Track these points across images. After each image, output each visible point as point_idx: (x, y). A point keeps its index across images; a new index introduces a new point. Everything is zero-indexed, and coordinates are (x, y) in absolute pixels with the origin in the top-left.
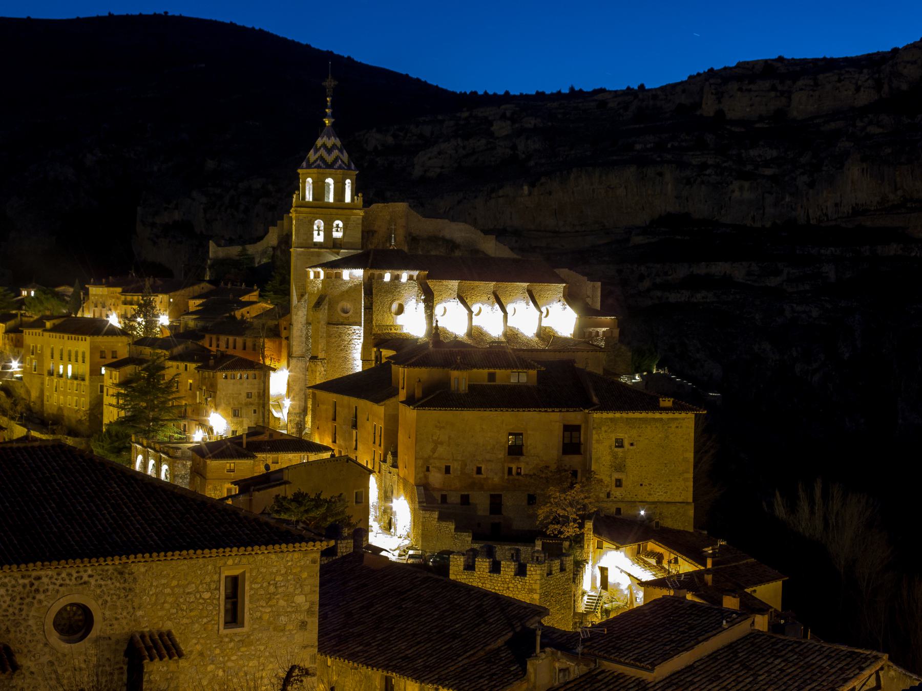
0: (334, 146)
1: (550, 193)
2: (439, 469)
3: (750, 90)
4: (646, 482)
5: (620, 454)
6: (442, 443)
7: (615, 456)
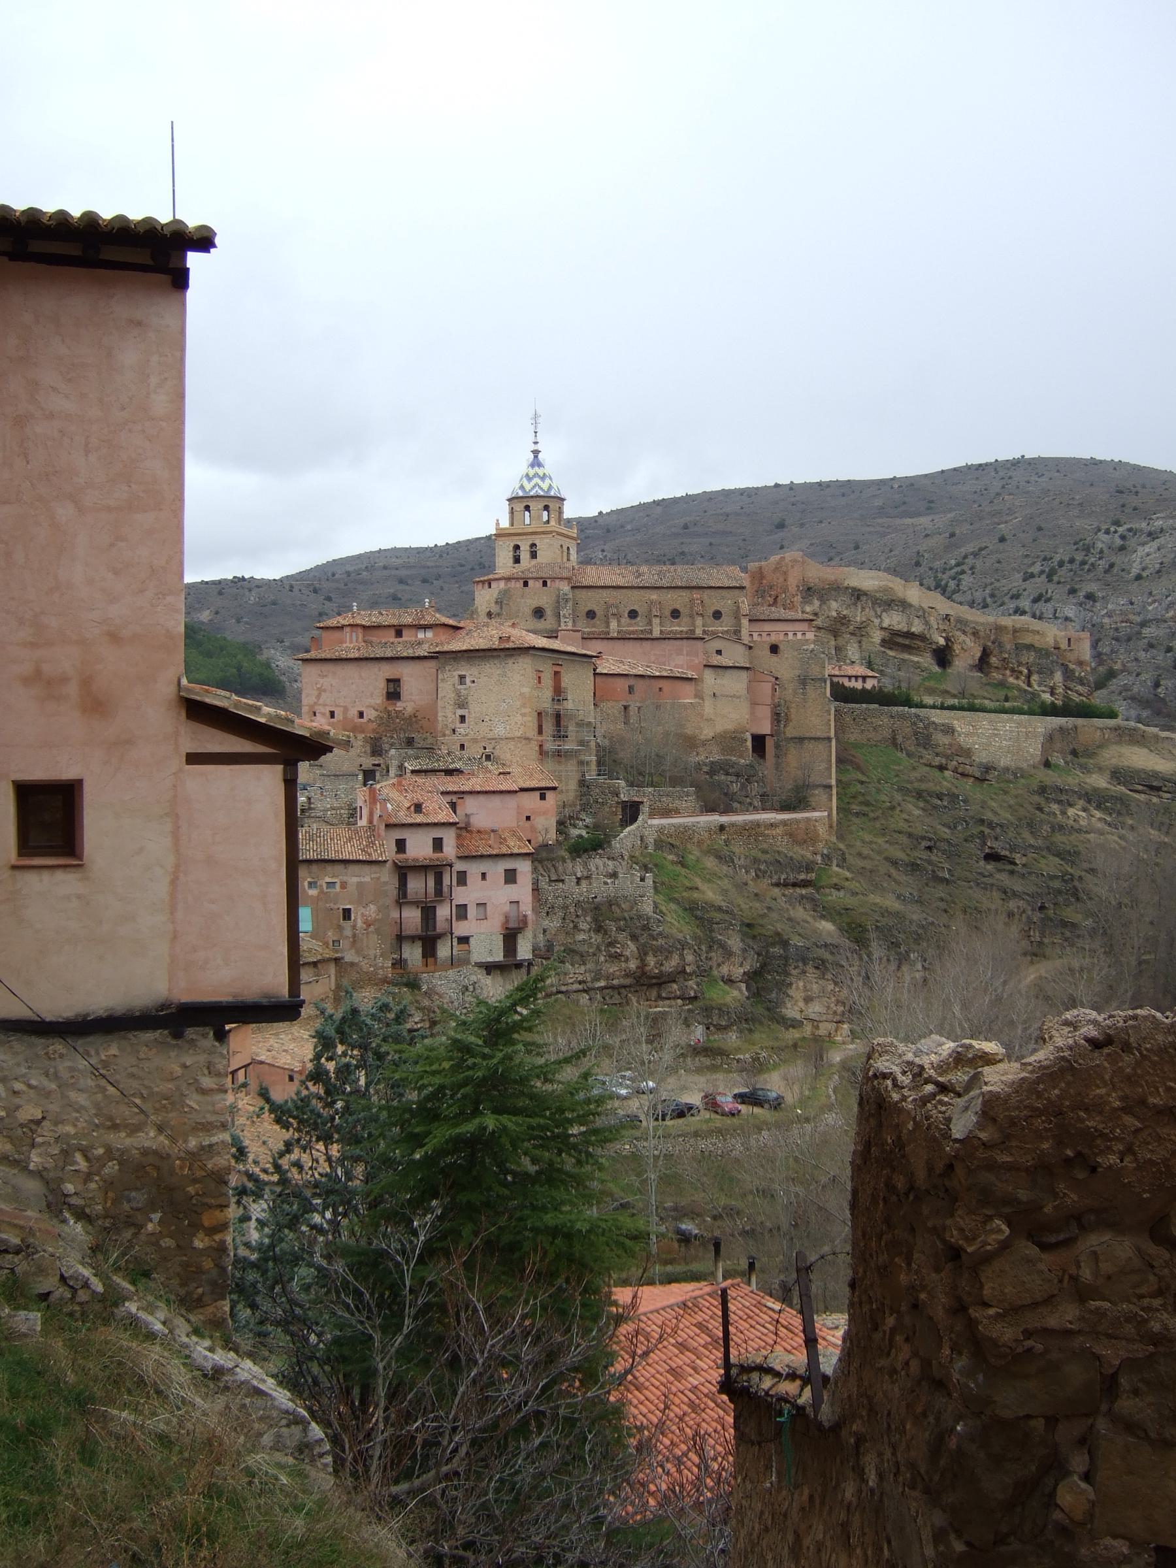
2: (323, 714)
4: (487, 718)
6: (325, 691)
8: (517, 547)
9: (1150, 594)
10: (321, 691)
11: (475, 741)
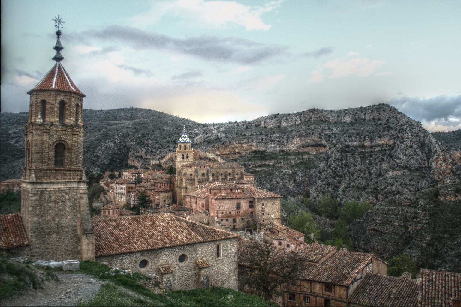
0: (186, 137)
1: (227, 146)
2: (220, 213)
3: (272, 121)
5: (263, 208)
7: (262, 208)
8: (183, 155)
9: (201, 148)
10: (220, 207)
11: (267, 219)
